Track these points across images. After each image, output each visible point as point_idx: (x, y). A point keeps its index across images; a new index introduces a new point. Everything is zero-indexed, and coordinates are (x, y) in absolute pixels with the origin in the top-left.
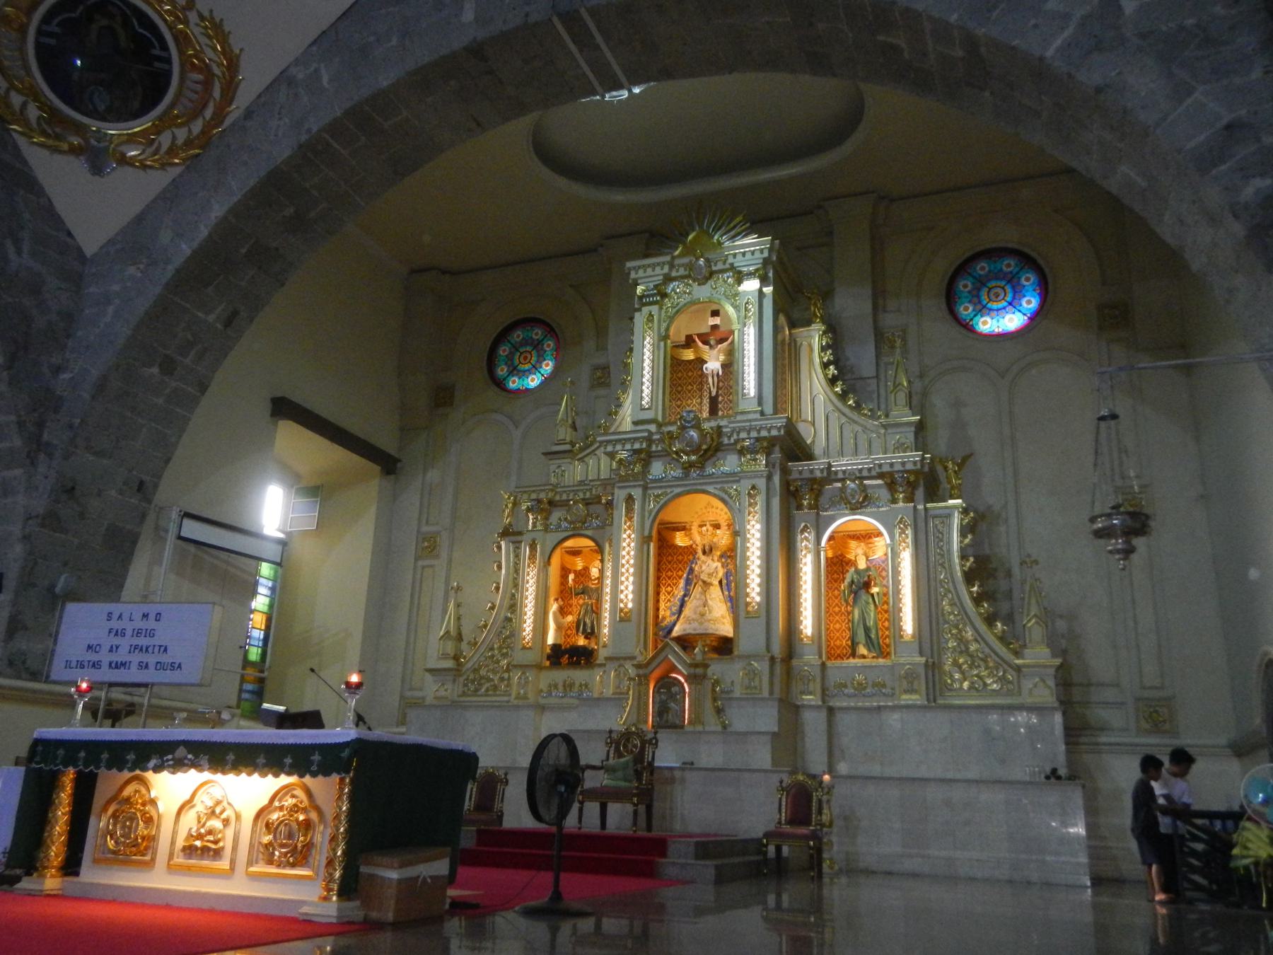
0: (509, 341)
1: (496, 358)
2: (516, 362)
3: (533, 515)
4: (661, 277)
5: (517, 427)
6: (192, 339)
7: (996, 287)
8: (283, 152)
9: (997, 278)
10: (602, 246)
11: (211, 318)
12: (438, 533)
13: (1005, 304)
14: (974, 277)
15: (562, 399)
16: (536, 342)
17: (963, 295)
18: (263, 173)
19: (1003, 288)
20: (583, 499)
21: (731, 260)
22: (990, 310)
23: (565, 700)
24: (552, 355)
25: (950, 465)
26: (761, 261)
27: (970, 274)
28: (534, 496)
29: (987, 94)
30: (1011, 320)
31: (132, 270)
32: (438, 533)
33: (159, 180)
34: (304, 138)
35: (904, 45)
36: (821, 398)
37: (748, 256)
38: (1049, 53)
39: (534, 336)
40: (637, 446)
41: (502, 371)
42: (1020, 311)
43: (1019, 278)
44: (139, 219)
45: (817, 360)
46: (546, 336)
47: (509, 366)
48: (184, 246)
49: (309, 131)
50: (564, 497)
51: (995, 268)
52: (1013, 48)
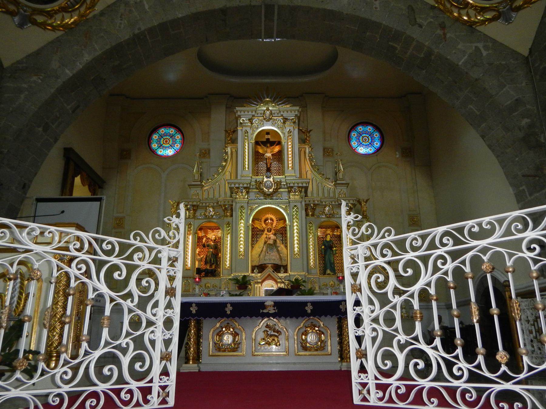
0: (158, 133)
1: (151, 139)
2: (162, 143)
3: (189, 211)
4: (251, 116)
5: (164, 172)
6: (58, 116)
8: (125, 35)
9: (365, 133)
10: (207, 97)
11: (69, 107)
12: (124, 217)
13: (369, 143)
14: (358, 132)
16: (171, 135)
17: (354, 138)
18: (114, 44)
19: (368, 137)
21: (282, 113)
22: (363, 145)
25: (363, 202)
26: (295, 115)
27: (356, 131)
28: (190, 203)
29: (424, 71)
30: (370, 150)
31: (34, 78)
32: (124, 217)
33: (51, 36)
34: (136, 32)
35: (399, 47)
36: (309, 172)
37: (289, 112)
38: (460, 63)
39: (170, 132)
40: (245, 185)
41: (154, 146)
42: (373, 147)
44: (38, 53)
45: (308, 158)
46: (176, 133)
47: (158, 144)
48: (67, 71)
49: (139, 29)
50: (204, 205)
51: (365, 129)
52: (447, 59)
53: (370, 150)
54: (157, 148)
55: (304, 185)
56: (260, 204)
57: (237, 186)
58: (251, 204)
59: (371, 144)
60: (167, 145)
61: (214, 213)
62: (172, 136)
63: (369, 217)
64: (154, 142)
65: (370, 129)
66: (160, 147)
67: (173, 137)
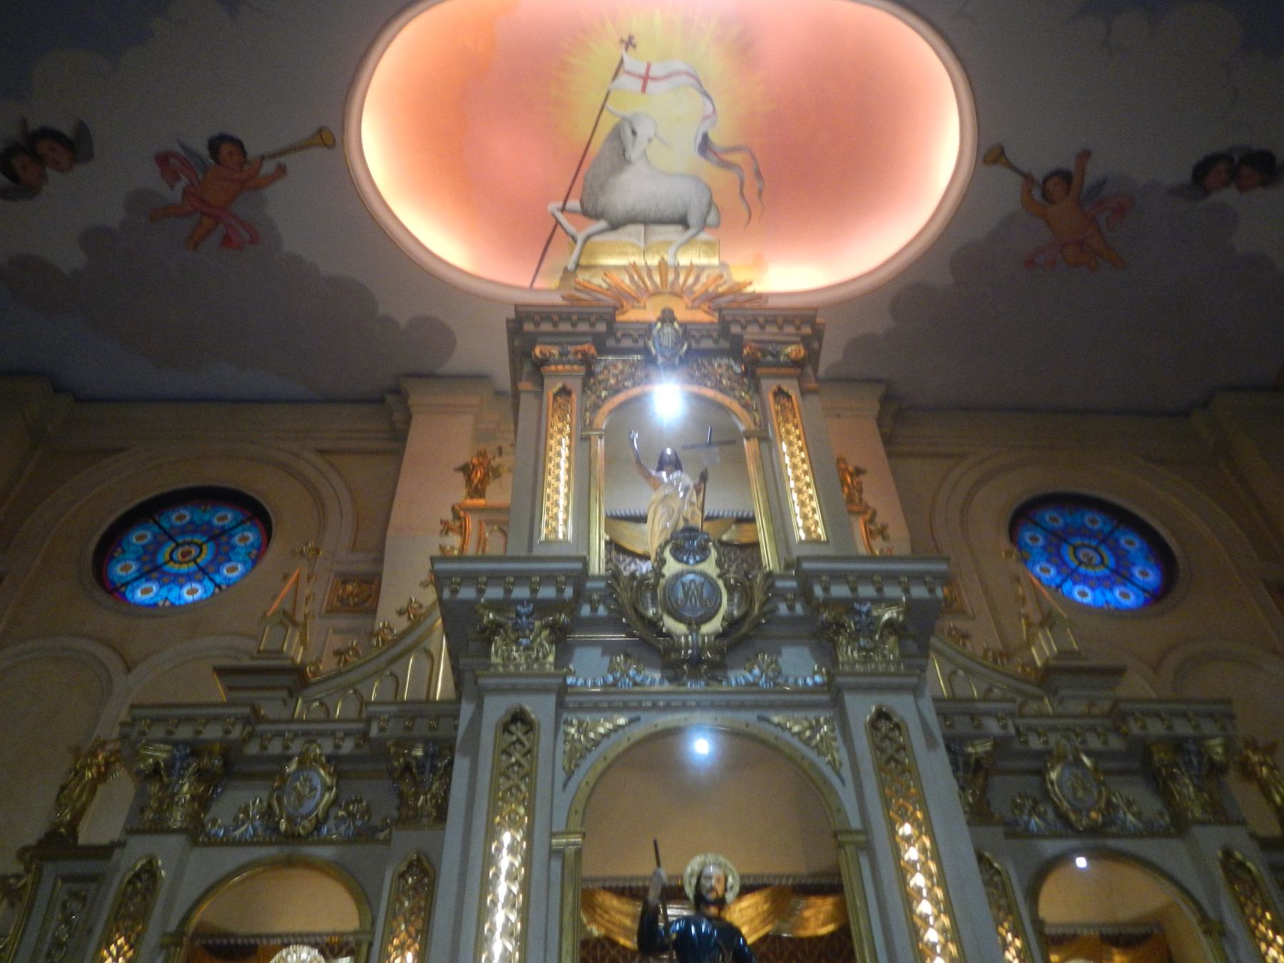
2: (163, 555)
5: (129, 670)
7: (1083, 546)
13: (1106, 571)
14: (1044, 529)
15: (286, 577)
19: (1096, 550)
21: (735, 329)
24: (249, 554)
28: (184, 733)
30: (1124, 595)
40: (547, 592)
43: (1117, 541)
46: (243, 522)
47: (144, 563)
50: (275, 748)
54: (129, 579)
55: (919, 592)
56: (640, 707)
57: (495, 593)
58: (581, 708)
59: (1121, 574)
60: (185, 568)
61: (335, 802)
62: (218, 537)
64: (129, 555)
65: (1095, 521)
66: (149, 572)
67: (224, 539)
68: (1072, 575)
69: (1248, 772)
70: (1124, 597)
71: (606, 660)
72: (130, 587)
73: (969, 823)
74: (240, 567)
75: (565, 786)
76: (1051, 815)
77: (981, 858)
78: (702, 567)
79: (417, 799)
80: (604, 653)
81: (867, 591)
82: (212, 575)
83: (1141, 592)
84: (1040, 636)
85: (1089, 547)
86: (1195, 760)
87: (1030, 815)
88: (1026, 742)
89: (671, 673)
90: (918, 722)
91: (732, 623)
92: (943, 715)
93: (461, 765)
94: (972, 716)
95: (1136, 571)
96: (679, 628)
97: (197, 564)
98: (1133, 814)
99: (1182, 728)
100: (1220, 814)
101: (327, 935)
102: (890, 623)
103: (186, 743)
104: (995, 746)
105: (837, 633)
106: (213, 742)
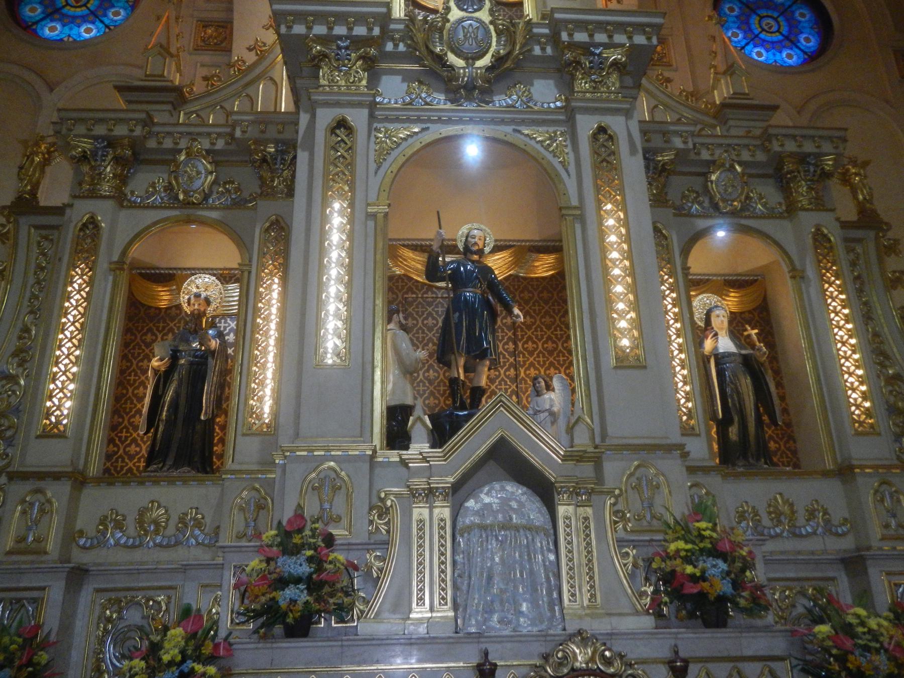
5: (52, 90)
7: (768, 16)
9: (768, 8)
13: (781, 37)
15: (159, 18)
19: (776, 19)
20: (208, 152)
22: (764, 41)
23: (138, 555)
28: (100, 130)
30: (789, 56)
40: (360, 31)
42: (797, 47)
43: (793, 12)
50: (168, 143)
53: (789, 56)
54: (37, 19)
55: (640, 39)
56: (429, 121)
57: (320, 30)
58: (387, 119)
59: (790, 40)
60: (79, 12)
61: (215, 182)
63: (886, 224)
68: (754, 39)
69: (846, 179)
70: (789, 58)
71: (405, 85)
72: (39, 26)
73: (651, 206)
74: (122, 12)
75: (376, 173)
76: (706, 204)
77: (656, 230)
78: (477, 15)
79: (273, 181)
80: (404, 80)
81: (601, 38)
82: (102, 19)
83: (801, 54)
84: (723, 81)
85: (771, 17)
86: (812, 169)
87: (693, 203)
88: (698, 154)
89: (452, 96)
90: (625, 134)
91: (499, 60)
92: (644, 133)
93: (302, 157)
94: (664, 134)
95: (802, 38)
96: (459, 62)
97: (88, 8)
98: (762, 205)
99: (809, 147)
100: (820, 204)
101: (221, 269)
102: (615, 63)
103: (103, 138)
104: (676, 155)
105: (576, 69)
106: (123, 137)
